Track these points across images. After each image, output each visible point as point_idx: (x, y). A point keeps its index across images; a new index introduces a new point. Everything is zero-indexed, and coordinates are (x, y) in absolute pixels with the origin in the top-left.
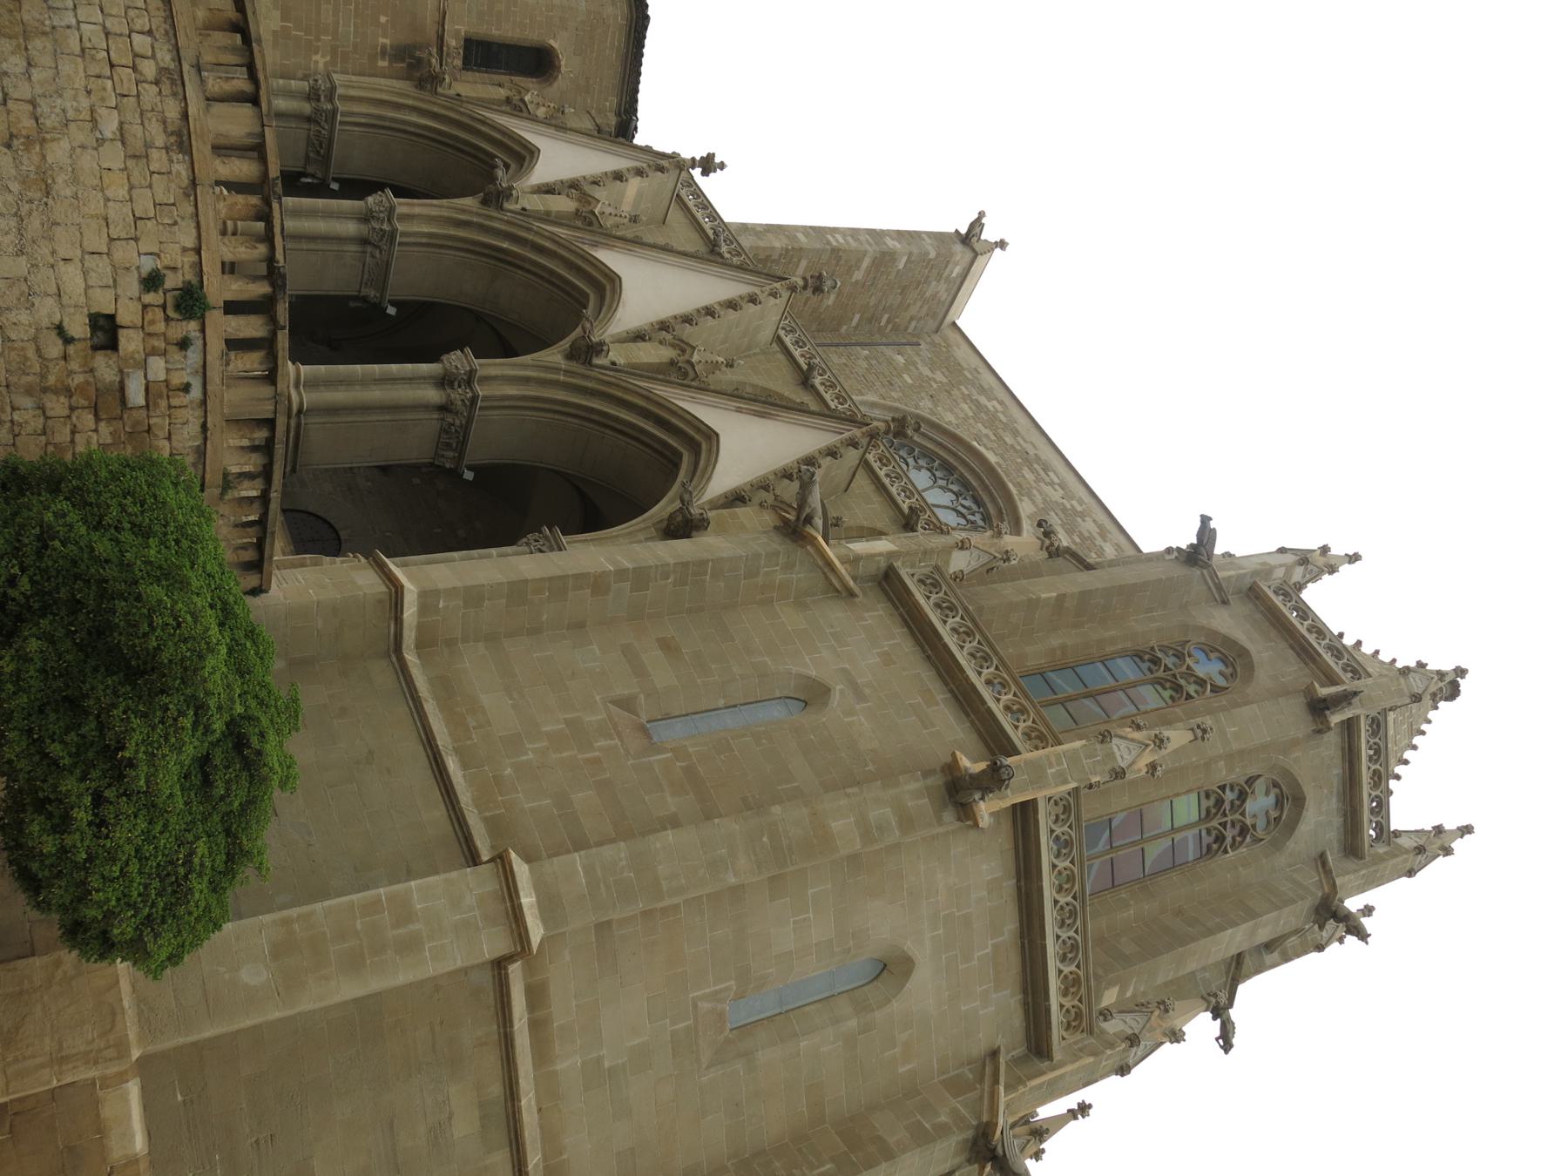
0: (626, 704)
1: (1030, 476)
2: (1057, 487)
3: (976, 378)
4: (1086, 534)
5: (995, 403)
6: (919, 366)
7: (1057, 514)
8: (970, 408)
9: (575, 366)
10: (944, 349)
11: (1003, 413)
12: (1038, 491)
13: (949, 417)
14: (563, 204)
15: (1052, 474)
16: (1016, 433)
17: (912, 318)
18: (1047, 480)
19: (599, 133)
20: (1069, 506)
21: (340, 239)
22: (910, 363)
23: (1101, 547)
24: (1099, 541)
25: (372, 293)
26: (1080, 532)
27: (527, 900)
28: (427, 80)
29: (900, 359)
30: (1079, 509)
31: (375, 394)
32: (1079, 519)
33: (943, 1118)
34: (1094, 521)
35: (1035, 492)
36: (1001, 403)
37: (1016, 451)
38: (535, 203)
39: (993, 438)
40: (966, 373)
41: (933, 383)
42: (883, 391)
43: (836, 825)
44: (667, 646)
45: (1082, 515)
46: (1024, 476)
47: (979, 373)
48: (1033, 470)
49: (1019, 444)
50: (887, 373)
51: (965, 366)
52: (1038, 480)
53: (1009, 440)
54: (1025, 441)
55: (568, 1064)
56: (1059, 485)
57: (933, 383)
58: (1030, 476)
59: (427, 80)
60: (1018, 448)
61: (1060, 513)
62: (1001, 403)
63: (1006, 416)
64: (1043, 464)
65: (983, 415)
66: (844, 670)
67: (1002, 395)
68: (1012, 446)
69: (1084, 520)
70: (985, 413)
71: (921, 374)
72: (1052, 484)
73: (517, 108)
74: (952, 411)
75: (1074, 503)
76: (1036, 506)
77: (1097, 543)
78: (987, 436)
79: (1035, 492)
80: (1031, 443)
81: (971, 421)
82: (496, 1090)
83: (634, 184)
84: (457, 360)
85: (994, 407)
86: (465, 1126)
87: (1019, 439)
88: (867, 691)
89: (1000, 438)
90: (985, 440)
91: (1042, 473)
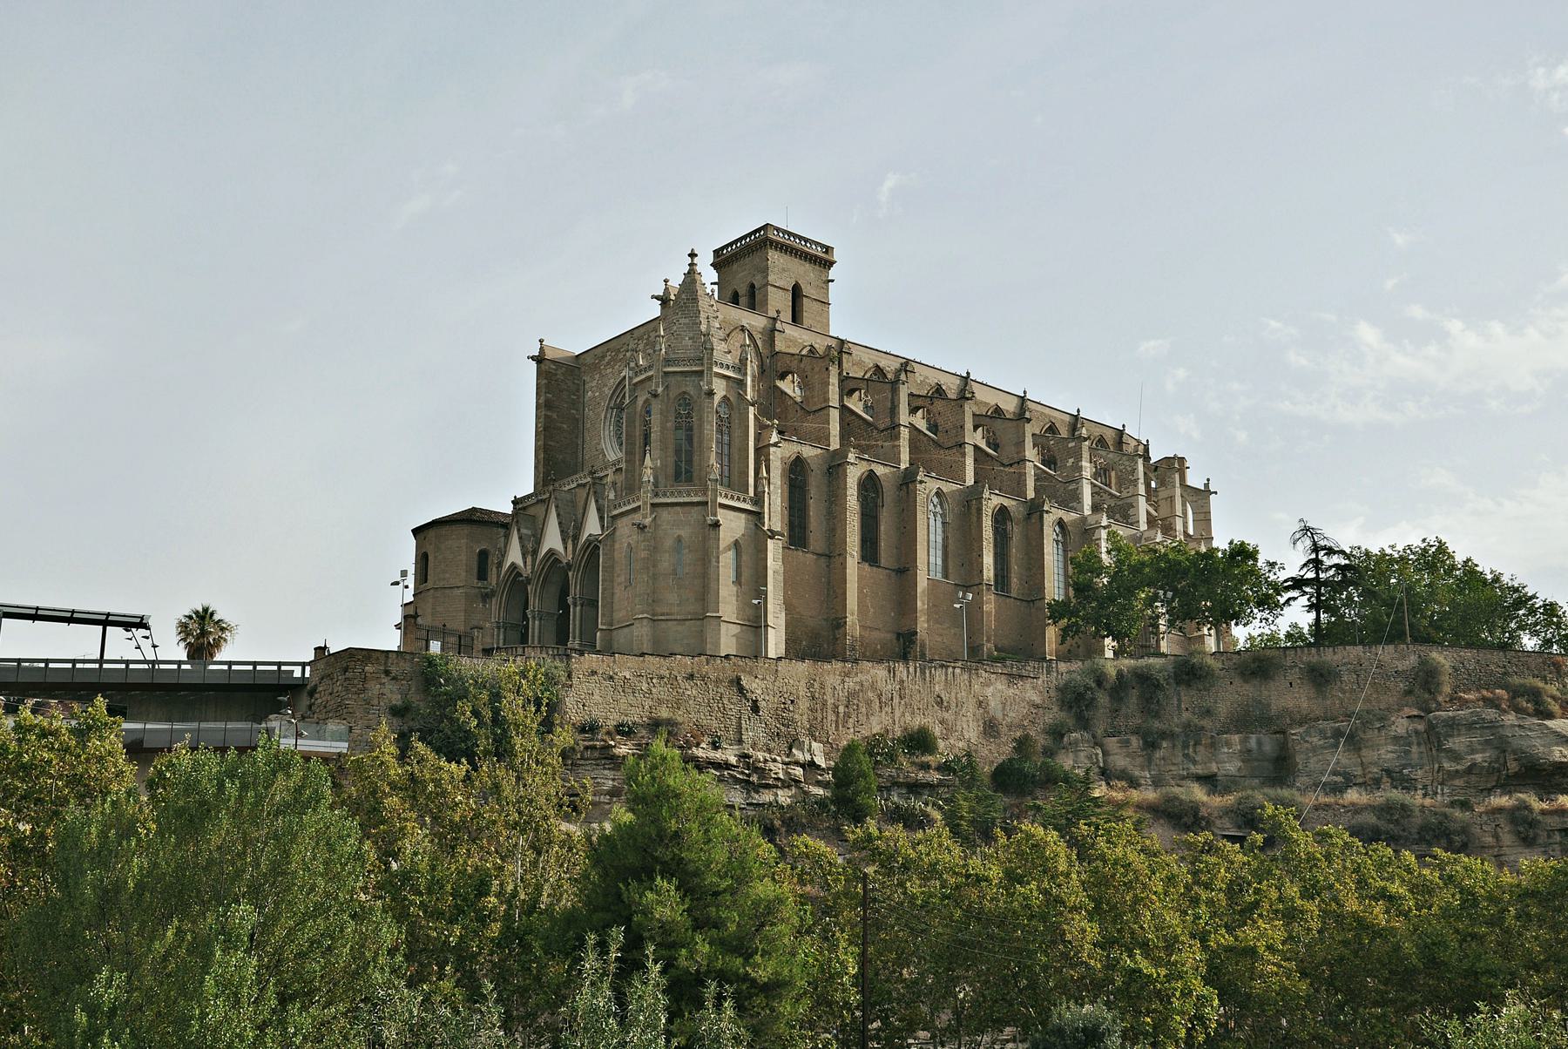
0: (626, 587)
9: (573, 569)
14: (529, 559)
17: (574, 383)
19: (507, 537)
21: (540, 625)
25: (556, 617)
27: (640, 616)
28: (493, 593)
31: (577, 623)
38: (529, 567)
44: (618, 576)
51: (593, 361)
55: (676, 609)
59: (493, 593)
67: (605, 348)
73: (500, 565)
82: (675, 623)
83: (524, 531)
84: (570, 600)
86: (679, 628)
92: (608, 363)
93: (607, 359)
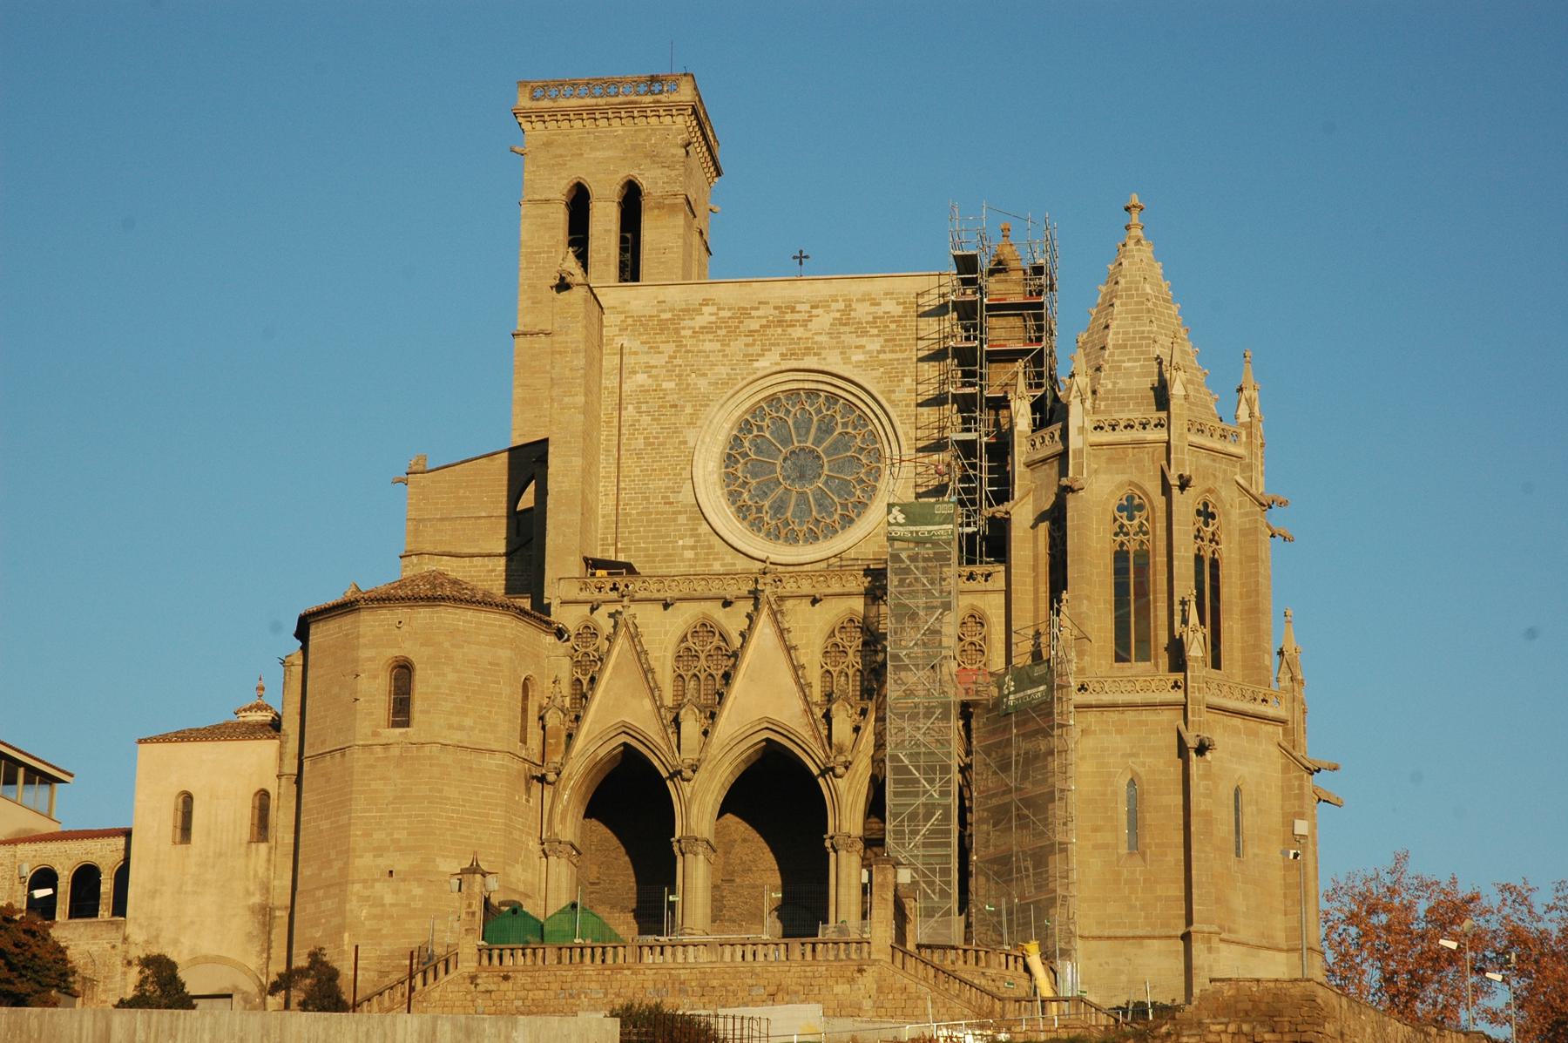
1: (798, 332)
2: (815, 312)
5: (705, 309)
6: (652, 362)
7: (844, 333)
8: (710, 341)
11: (719, 309)
12: (816, 334)
13: (723, 371)
15: (799, 307)
16: (744, 313)
20: (838, 315)
22: (648, 368)
23: (885, 313)
24: (880, 311)
26: (867, 323)
29: (641, 378)
30: (841, 305)
33: (1296, 783)
35: (817, 338)
36: (706, 302)
40: (664, 316)
41: (676, 362)
43: (1203, 807)
45: (849, 307)
46: (799, 339)
49: (759, 317)
53: (755, 325)
54: (757, 309)
56: (812, 307)
57: (676, 362)
58: (798, 332)
60: (764, 322)
62: (706, 302)
63: (724, 309)
64: (787, 307)
65: (722, 332)
66: (1123, 755)
68: (761, 327)
69: (855, 310)
70: (720, 328)
71: (662, 367)
75: (834, 306)
76: (834, 348)
77: (882, 315)
78: (747, 345)
79: (817, 338)
80: (760, 303)
85: (711, 314)
87: (754, 313)
88: (1134, 750)
89: (751, 333)
90: (751, 350)
91: (796, 316)
92: (705, 329)
93: (700, 321)
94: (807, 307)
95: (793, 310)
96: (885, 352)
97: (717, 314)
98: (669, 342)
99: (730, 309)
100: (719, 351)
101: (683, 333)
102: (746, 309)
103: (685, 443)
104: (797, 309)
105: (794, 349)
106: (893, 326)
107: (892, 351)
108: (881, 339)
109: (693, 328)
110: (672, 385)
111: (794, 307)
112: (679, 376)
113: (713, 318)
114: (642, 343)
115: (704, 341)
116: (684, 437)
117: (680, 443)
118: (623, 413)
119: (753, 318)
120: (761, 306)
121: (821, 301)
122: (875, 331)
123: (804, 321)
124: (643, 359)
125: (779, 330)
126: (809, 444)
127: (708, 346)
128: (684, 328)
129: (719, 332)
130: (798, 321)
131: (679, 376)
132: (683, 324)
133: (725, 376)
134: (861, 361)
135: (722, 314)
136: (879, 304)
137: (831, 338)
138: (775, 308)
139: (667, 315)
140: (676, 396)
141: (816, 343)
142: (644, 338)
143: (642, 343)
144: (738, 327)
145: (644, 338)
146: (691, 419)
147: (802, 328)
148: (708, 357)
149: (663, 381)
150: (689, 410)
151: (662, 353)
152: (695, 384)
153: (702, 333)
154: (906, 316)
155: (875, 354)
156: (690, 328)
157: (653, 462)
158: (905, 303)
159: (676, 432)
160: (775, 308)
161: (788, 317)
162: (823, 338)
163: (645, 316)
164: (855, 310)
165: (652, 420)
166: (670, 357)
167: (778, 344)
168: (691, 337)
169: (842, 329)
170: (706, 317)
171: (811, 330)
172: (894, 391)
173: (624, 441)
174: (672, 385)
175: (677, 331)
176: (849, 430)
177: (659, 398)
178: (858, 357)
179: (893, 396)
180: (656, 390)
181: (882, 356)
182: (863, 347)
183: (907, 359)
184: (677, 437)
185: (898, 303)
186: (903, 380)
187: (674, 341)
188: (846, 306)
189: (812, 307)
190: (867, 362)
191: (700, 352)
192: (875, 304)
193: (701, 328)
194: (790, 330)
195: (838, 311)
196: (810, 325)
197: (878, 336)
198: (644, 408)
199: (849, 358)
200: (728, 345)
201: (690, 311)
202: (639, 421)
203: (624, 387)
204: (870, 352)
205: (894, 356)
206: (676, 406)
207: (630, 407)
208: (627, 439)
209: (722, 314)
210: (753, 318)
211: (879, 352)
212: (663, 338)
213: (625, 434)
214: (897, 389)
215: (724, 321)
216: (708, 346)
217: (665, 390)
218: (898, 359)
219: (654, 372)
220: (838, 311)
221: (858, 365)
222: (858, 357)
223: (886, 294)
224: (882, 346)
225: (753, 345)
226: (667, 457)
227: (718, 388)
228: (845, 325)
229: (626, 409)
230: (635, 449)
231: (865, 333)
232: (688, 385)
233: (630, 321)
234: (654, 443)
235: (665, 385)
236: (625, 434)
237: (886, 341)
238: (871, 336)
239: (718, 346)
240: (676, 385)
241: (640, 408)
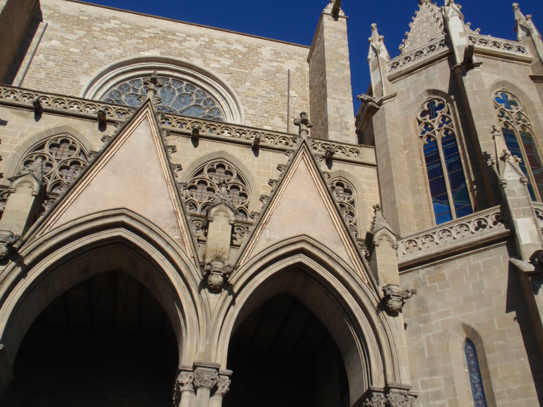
1: (175, 45)
2: (188, 38)
3: (88, 16)
4: (226, 49)
7: (208, 52)
8: (112, 36)
10: (57, 15)
11: (122, 23)
13: (117, 51)
15: (177, 34)
18: (182, 39)
20: (204, 43)
24: (232, 47)
26: (223, 51)
30: (207, 40)
32: (214, 45)
34: (217, 39)
35: (187, 50)
36: (114, 18)
37: (154, 38)
39: (141, 41)
40: (81, 18)
41: (83, 40)
42: (80, 70)
46: (175, 48)
47: (85, 12)
48: (172, 40)
50: (66, 57)
51: (76, 14)
52: (180, 42)
53: (146, 36)
54: (149, 29)
56: (186, 36)
58: (175, 45)
60: (152, 35)
61: (207, 50)
62: (114, 18)
64: (170, 32)
65: (121, 34)
68: (150, 37)
69: (216, 43)
72: (185, 40)
74: (111, 47)
75: (201, 38)
77: (233, 49)
78: (137, 43)
79: (187, 50)
80: (151, 26)
81: (123, 43)
87: (145, 30)
89: (142, 38)
90: (140, 46)
94: (184, 35)
95: (174, 34)
96: (233, 67)
97: (121, 25)
98: (81, 30)
99: (129, 24)
100: (117, 42)
101: (93, 28)
102: (142, 27)
103: (78, 82)
104: (176, 35)
105: (171, 52)
106: (241, 56)
107: (239, 68)
108: (232, 61)
109: (103, 28)
110: (78, 51)
111: (175, 34)
112: (84, 48)
113: (117, 26)
114: (62, 26)
115: (108, 35)
116: (79, 79)
117: (74, 81)
118: (35, 57)
119: (145, 32)
120: (152, 28)
121: (193, 34)
122: (228, 56)
123: (180, 41)
124: (59, 34)
125: (162, 41)
126: (170, 106)
127: (109, 38)
128: (95, 26)
129: (119, 33)
130: (177, 40)
131: (84, 48)
132: (94, 24)
133: (118, 54)
134: (217, 68)
135: (123, 25)
136: (232, 44)
137: (198, 53)
138: (161, 31)
139: (86, 18)
140: (78, 57)
141: (187, 52)
142: (64, 24)
143: (62, 26)
144: (134, 34)
145: (64, 24)
146: (87, 71)
147: (178, 44)
148: (109, 43)
149: (71, 47)
150: (86, 65)
151: (76, 34)
152: (96, 54)
153: (107, 31)
154: (250, 54)
155: (227, 66)
156: (99, 27)
157: (48, 87)
158: (249, 48)
159: (70, 75)
160: (161, 31)
161: (170, 37)
162: (193, 52)
163: (68, 15)
164: (216, 43)
165: (56, 65)
166: (80, 37)
167: (160, 48)
168: (98, 31)
169: (206, 50)
170: (113, 24)
171: (184, 46)
172: (238, 87)
173: (30, 71)
174: (78, 51)
175: (90, 27)
176: (202, 104)
177: (65, 55)
178: (216, 65)
179: (237, 89)
180: (64, 51)
181: (231, 68)
182: (219, 61)
183: (248, 73)
184: (72, 78)
185: (245, 47)
186: (245, 83)
187: (85, 30)
188: (210, 40)
189: (186, 36)
190: (220, 68)
191: (104, 39)
192: (228, 43)
193: (106, 28)
194: (169, 43)
195: (204, 41)
196: (183, 44)
197: (231, 59)
198: (52, 57)
199: (209, 64)
200: (125, 41)
201: (100, 19)
202: (45, 64)
203: (41, 44)
204: (222, 64)
205: (239, 70)
206: (76, 62)
207: (41, 56)
208: (33, 71)
209: (123, 25)
210: (145, 32)
211: (229, 66)
212: (79, 27)
213: (31, 68)
214: (240, 86)
215: (124, 29)
216: (109, 38)
217: (71, 52)
218: (243, 72)
219: (66, 41)
220: (204, 41)
221: (214, 68)
222: (216, 65)
223: (237, 41)
224: (231, 64)
225: (142, 44)
226: (61, 87)
227: (111, 59)
228: (208, 48)
229: (38, 55)
230: (37, 78)
231: (221, 55)
232: (90, 53)
233: (57, 15)
234: (53, 78)
235: (72, 50)
236: (31, 68)
237: (235, 62)
238: (224, 57)
239: (117, 39)
240: (81, 51)
241: (49, 57)
